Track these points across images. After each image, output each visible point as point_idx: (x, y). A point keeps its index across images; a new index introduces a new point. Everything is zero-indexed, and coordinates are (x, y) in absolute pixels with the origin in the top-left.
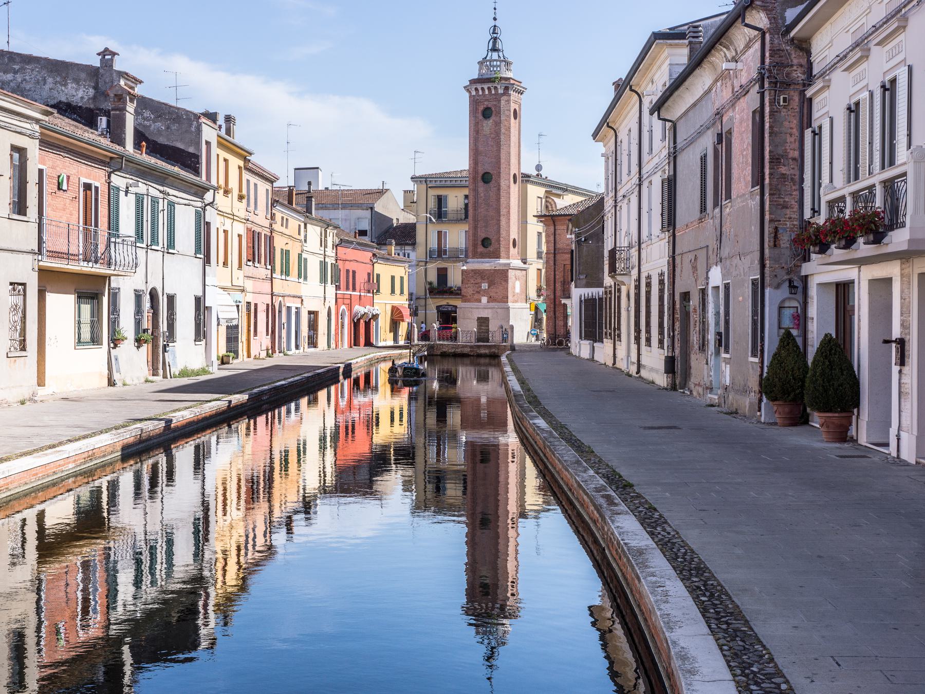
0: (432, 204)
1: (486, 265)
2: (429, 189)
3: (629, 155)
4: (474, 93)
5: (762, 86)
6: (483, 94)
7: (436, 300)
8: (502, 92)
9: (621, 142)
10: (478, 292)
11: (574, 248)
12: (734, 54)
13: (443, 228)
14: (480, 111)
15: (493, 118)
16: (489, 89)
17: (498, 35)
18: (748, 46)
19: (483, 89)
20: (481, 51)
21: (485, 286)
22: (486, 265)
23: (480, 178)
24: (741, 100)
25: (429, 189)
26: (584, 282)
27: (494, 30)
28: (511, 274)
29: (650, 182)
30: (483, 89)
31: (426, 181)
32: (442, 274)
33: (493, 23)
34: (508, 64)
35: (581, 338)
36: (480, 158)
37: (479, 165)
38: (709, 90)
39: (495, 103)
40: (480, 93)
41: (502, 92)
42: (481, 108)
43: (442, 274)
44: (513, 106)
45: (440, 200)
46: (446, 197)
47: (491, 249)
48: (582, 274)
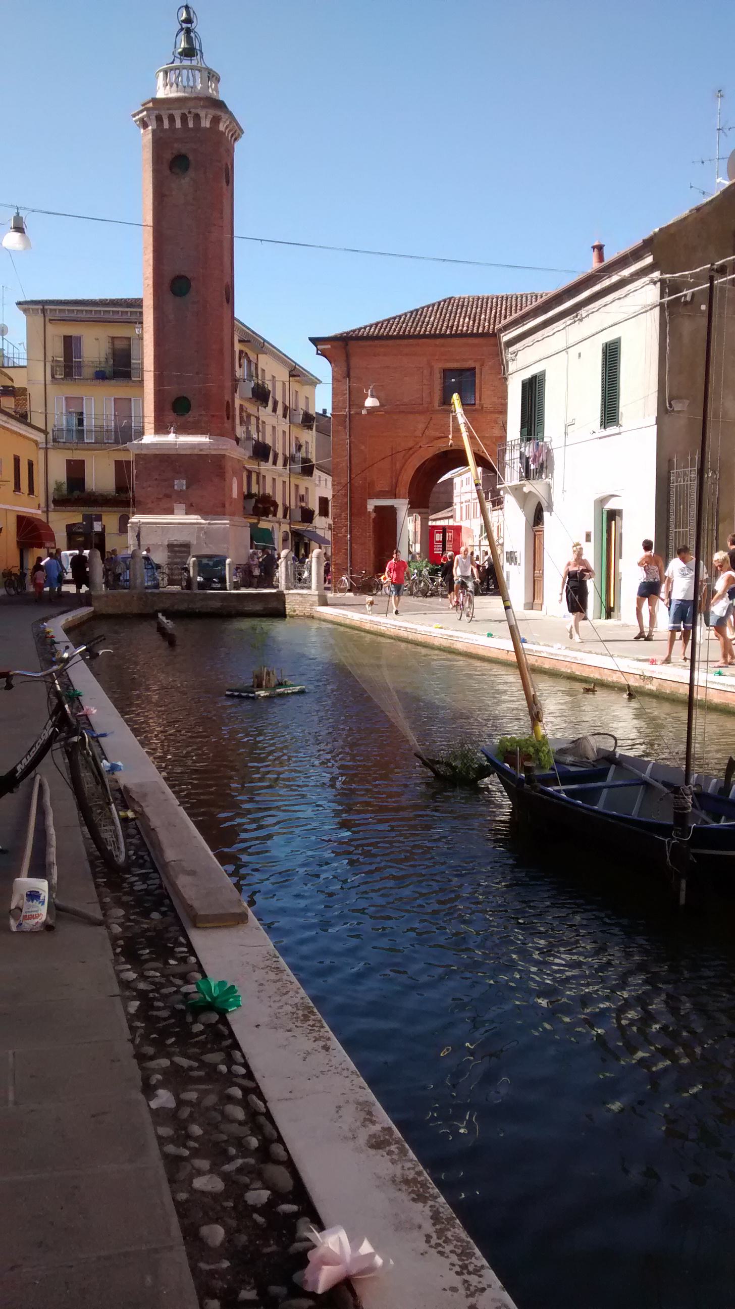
0: (57, 350)
2: (49, 326)
7: (65, 515)
8: (208, 125)
10: (168, 496)
13: (73, 390)
15: (191, 173)
16: (184, 118)
19: (172, 118)
25: (49, 326)
30: (172, 118)
31: (44, 311)
32: (76, 470)
34: (212, 76)
41: (208, 125)
42: (168, 156)
43: (76, 470)
46: (79, 339)
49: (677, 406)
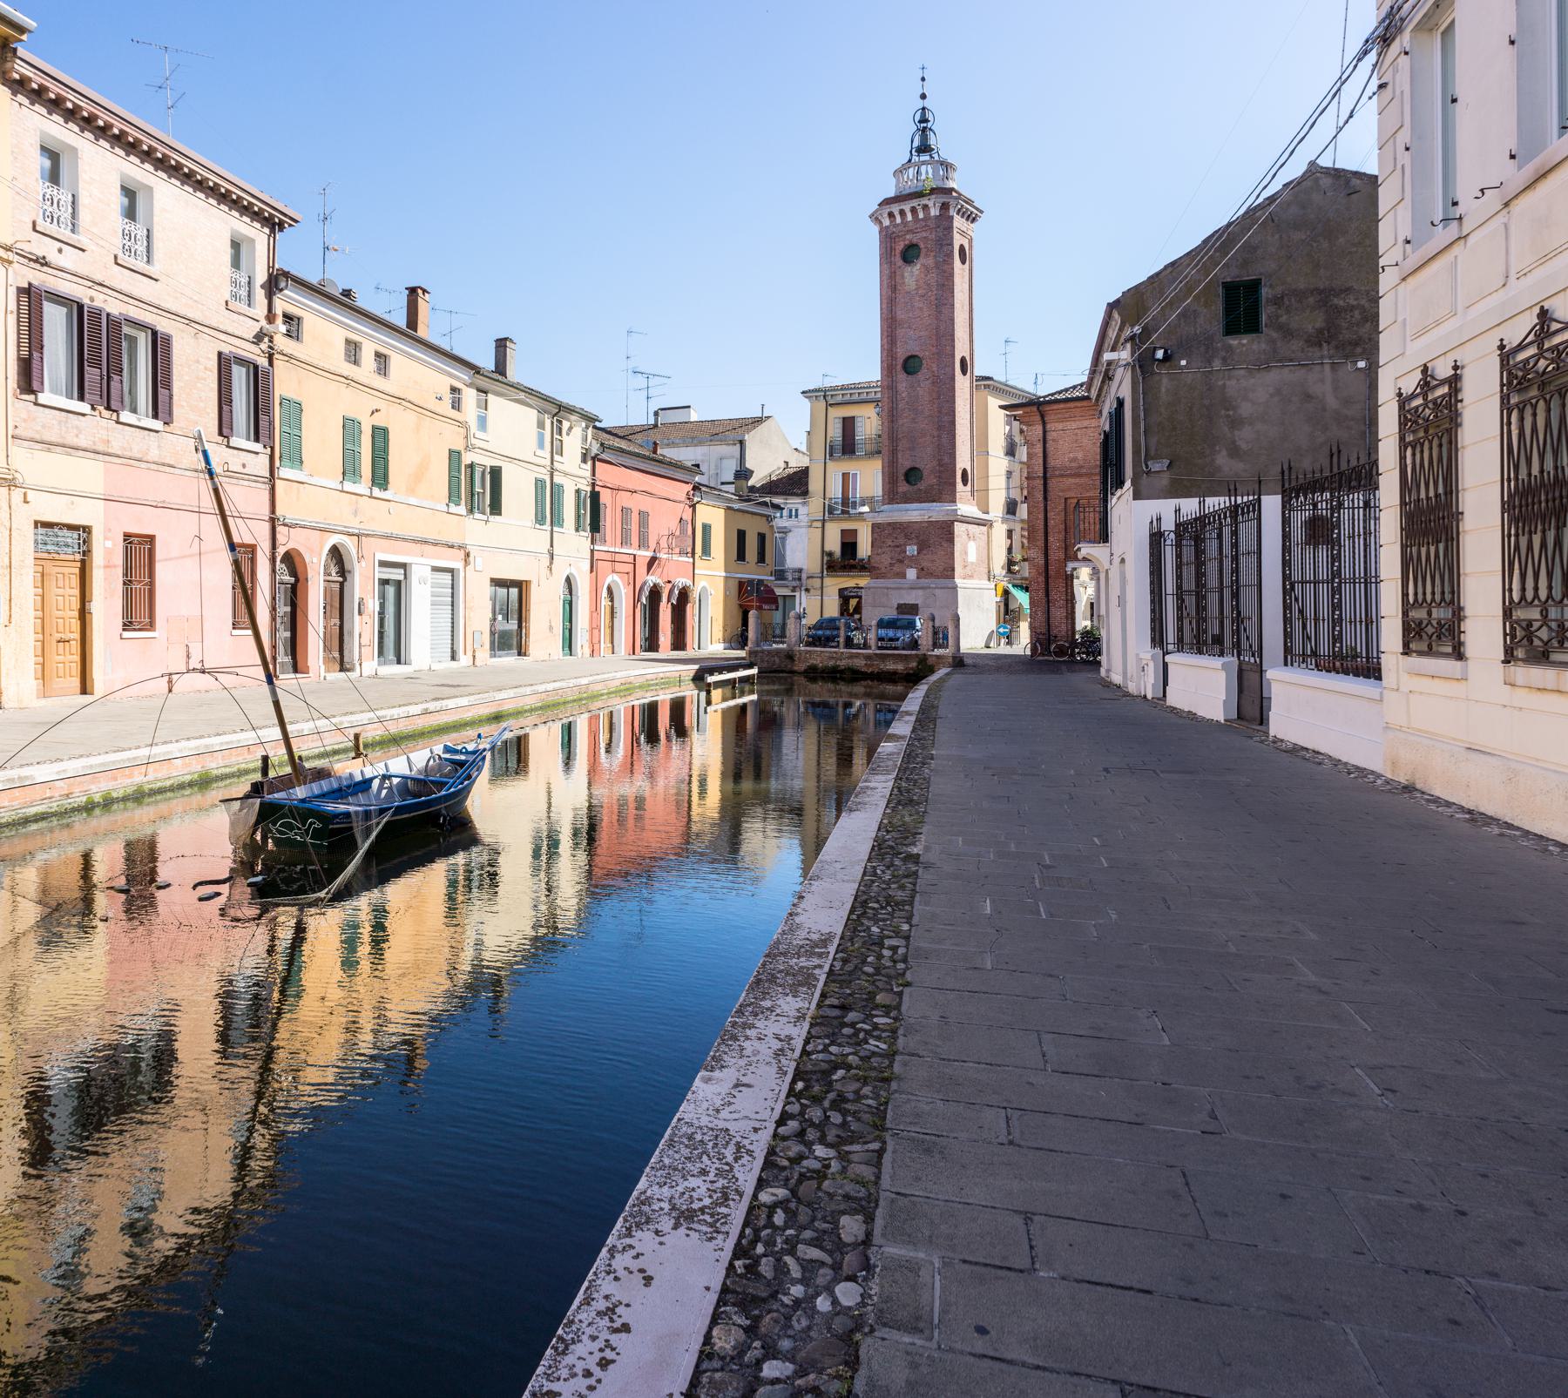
1: (914, 513)
4: (886, 222)
6: (902, 223)
8: (938, 214)
10: (901, 561)
11: (1126, 392)
14: (898, 252)
15: (922, 260)
16: (914, 210)
17: (929, 125)
19: (902, 213)
20: (900, 148)
21: (912, 550)
22: (914, 513)
23: (899, 367)
26: (1164, 480)
27: (923, 114)
28: (959, 529)
30: (902, 213)
33: (920, 103)
35: (1158, 639)
36: (900, 332)
37: (899, 344)
39: (924, 234)
40: (898, 220)
42: (900, 246)
44: (958, 240)
45: (848, 424)
47: (922, 486)
48: (1157, 457)
49: (1155, 466)
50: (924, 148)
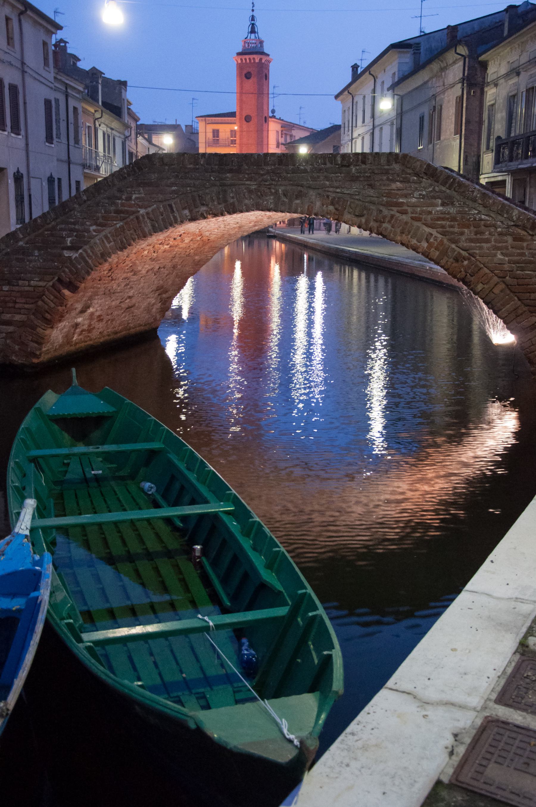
0: (210, 135)
3: (364, 111)
4: (239, 61)
5: (463, 85)
9: (357, 102)
12: (445, 65)
14: (244, 74)
16: (250, 59)
18: (454, 63)
19: (246, 59)
24: (449, 90)
29: (381, 129)
30: (246, 59)
33: (251, 14)
38: (428, 81)
42: (245, 72)
50: (253, 31)
